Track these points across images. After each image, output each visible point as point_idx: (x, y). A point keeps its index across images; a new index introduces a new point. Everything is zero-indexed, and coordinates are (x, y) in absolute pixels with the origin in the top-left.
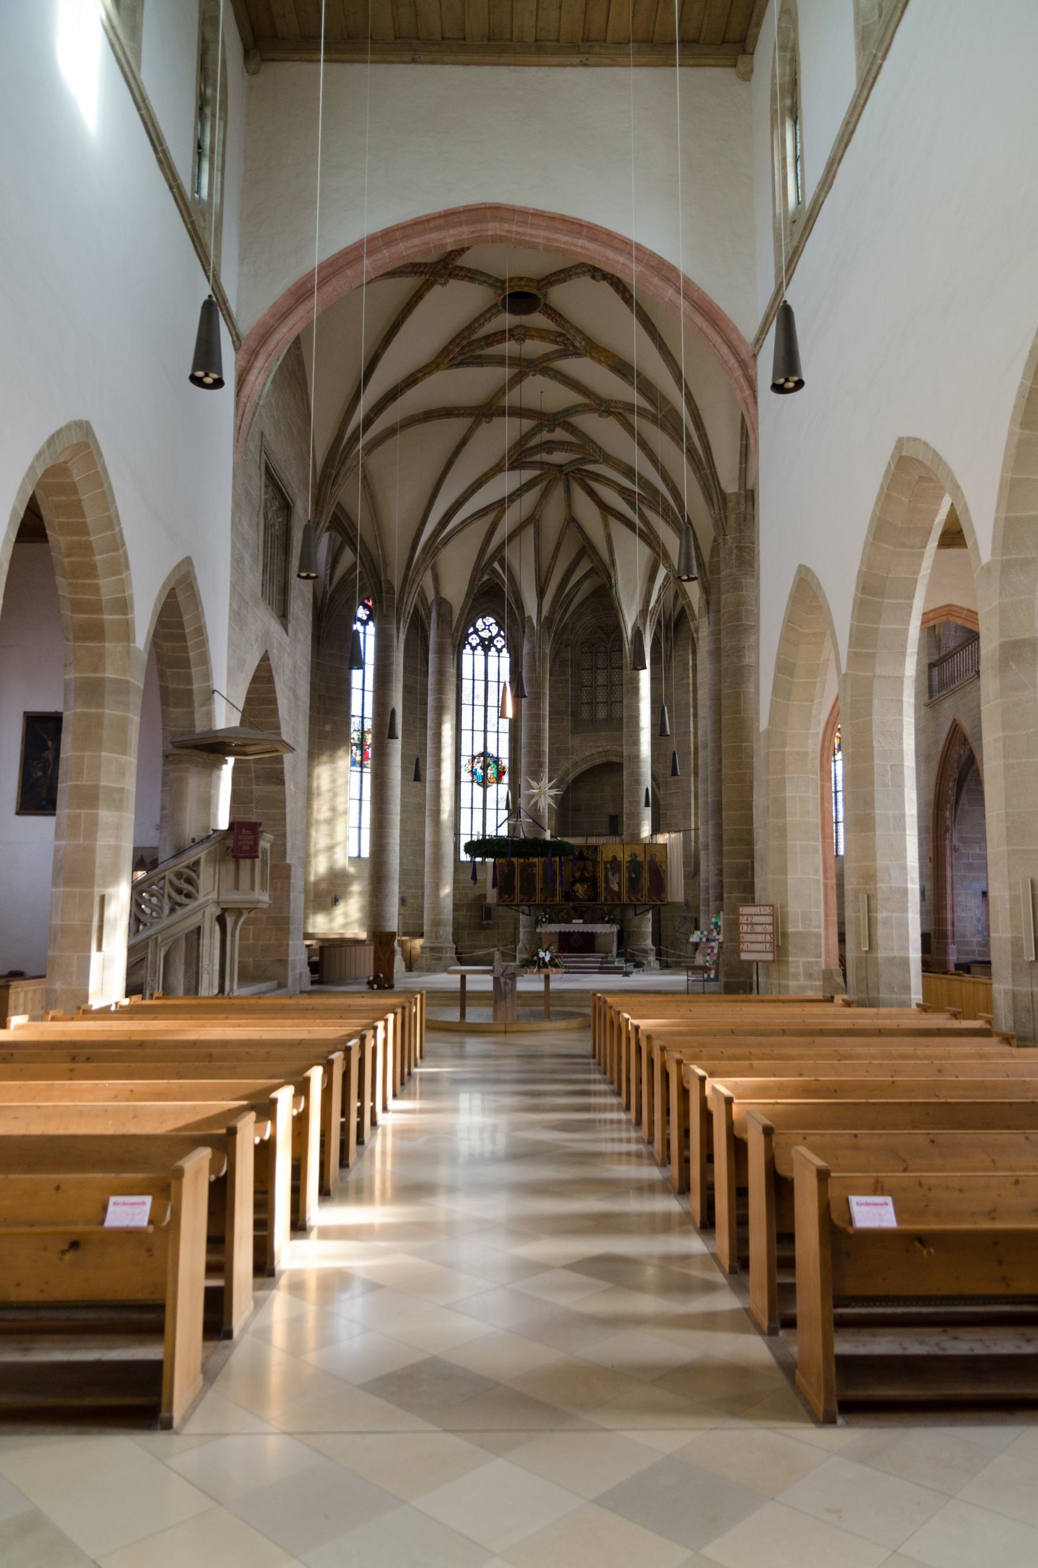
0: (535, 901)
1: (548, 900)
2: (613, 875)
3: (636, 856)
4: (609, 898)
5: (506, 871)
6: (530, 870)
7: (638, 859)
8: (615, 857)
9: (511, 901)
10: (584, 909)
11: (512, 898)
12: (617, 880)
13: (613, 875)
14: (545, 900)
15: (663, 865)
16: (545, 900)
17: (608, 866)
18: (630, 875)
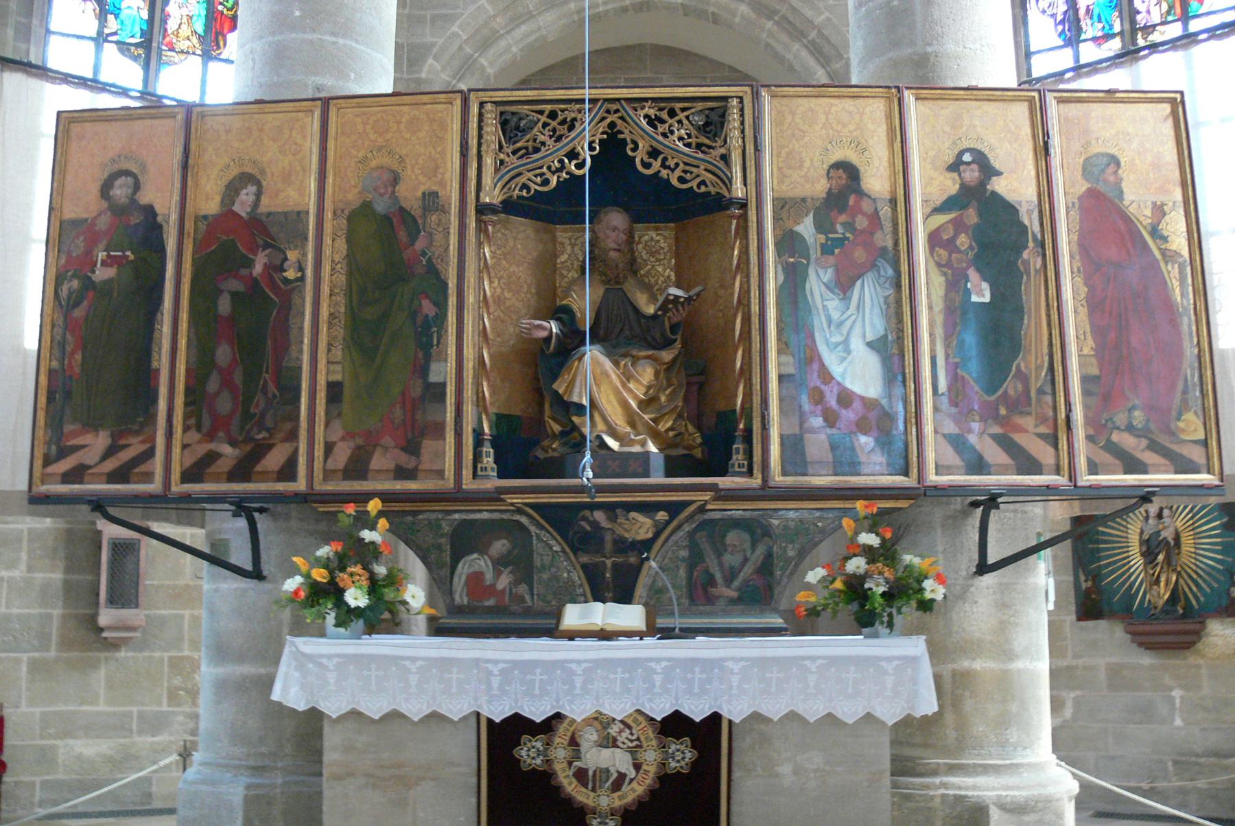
0: (288, 472)
1: (379, 461)
2: (843, 285)
3: (988, 170)
4: (817, 444)
5: (102, 274)
6: (260, 263)
7: (999, 186)
8: (847, 174)
9: (120, 475)
10: (641, 527)
11: (135, 447)
12: (873, 323)
13: (843, 285)
14: (357, 468)
15: (1176, 226)
16: (357, 468)
17: (806, 228)
18: (956, 284)
